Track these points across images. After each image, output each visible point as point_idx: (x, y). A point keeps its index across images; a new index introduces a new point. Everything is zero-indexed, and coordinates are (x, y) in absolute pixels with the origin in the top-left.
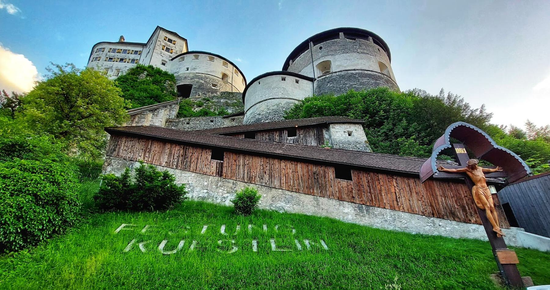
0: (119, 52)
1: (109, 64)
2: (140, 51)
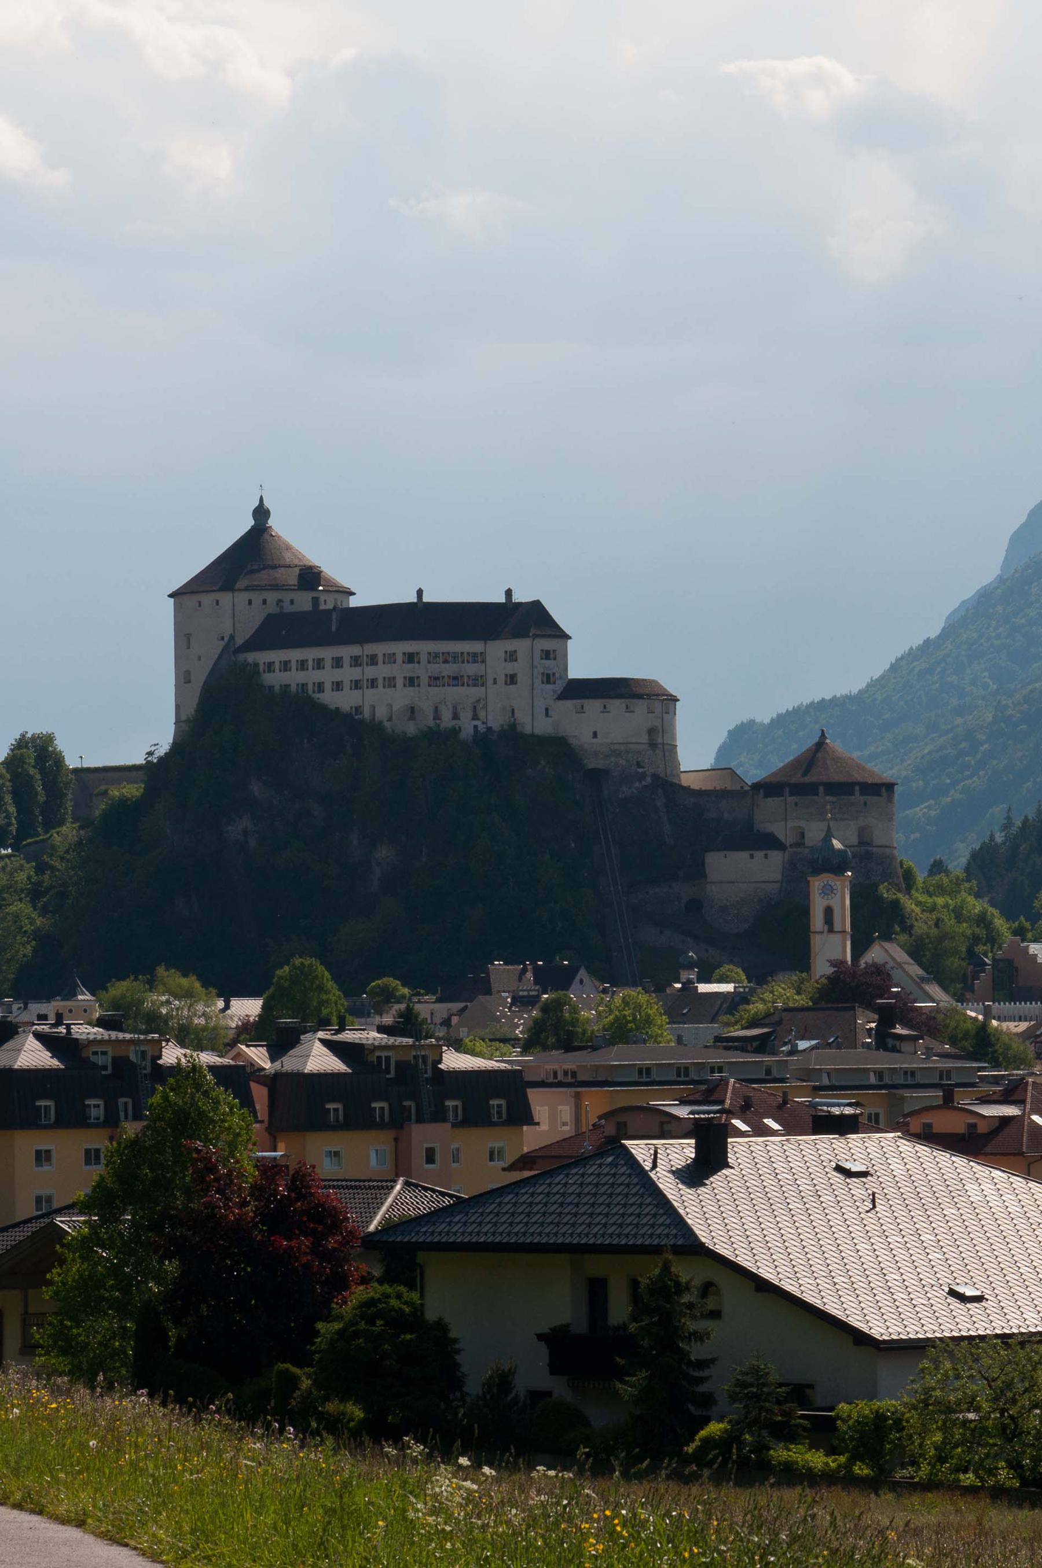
0: (446, 661)
1: (437, 693)
2: (481, 653)
